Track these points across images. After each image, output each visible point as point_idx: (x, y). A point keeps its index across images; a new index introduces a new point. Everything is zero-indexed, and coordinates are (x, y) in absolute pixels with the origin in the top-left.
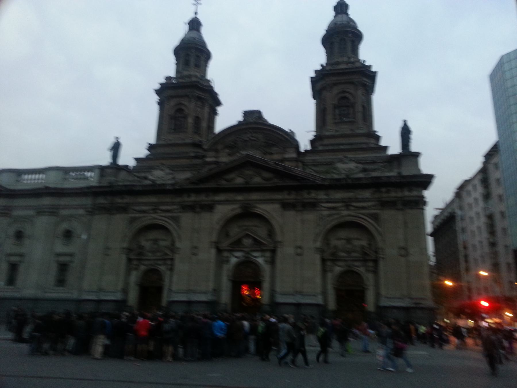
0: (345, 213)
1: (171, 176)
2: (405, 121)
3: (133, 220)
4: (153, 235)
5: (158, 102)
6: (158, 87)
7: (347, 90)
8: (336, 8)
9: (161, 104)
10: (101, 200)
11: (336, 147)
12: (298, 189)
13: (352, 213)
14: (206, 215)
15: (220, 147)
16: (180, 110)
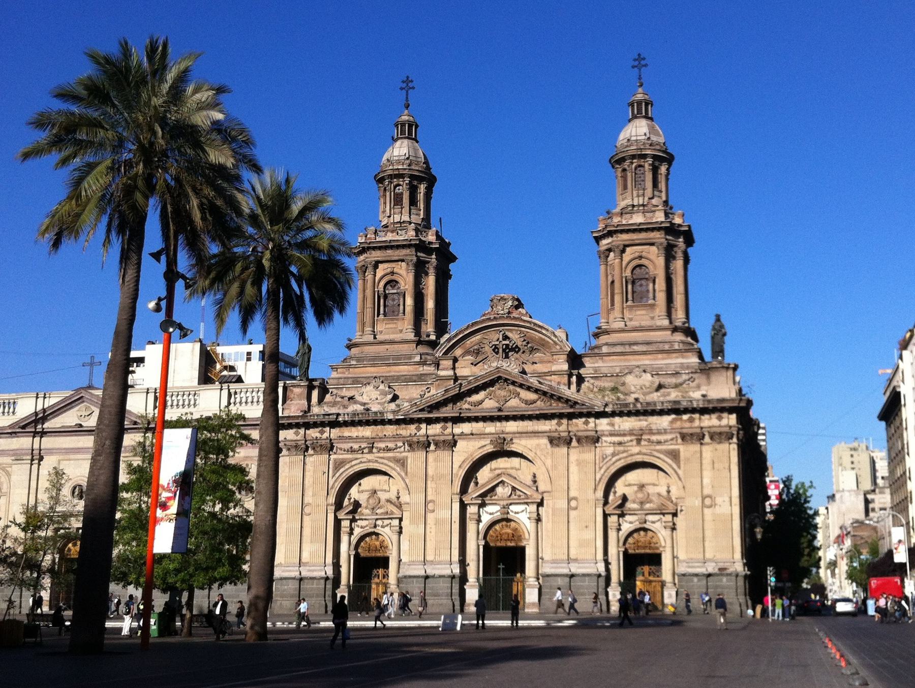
0: (636, 449)
1: (390, 397)
3: (339, 465)
4: (368, 482)
7: (644, 254)
11: (627, 349)
12: (570, 416)
13: (644, 451)
14: (444, 455)
15: (458, 352)
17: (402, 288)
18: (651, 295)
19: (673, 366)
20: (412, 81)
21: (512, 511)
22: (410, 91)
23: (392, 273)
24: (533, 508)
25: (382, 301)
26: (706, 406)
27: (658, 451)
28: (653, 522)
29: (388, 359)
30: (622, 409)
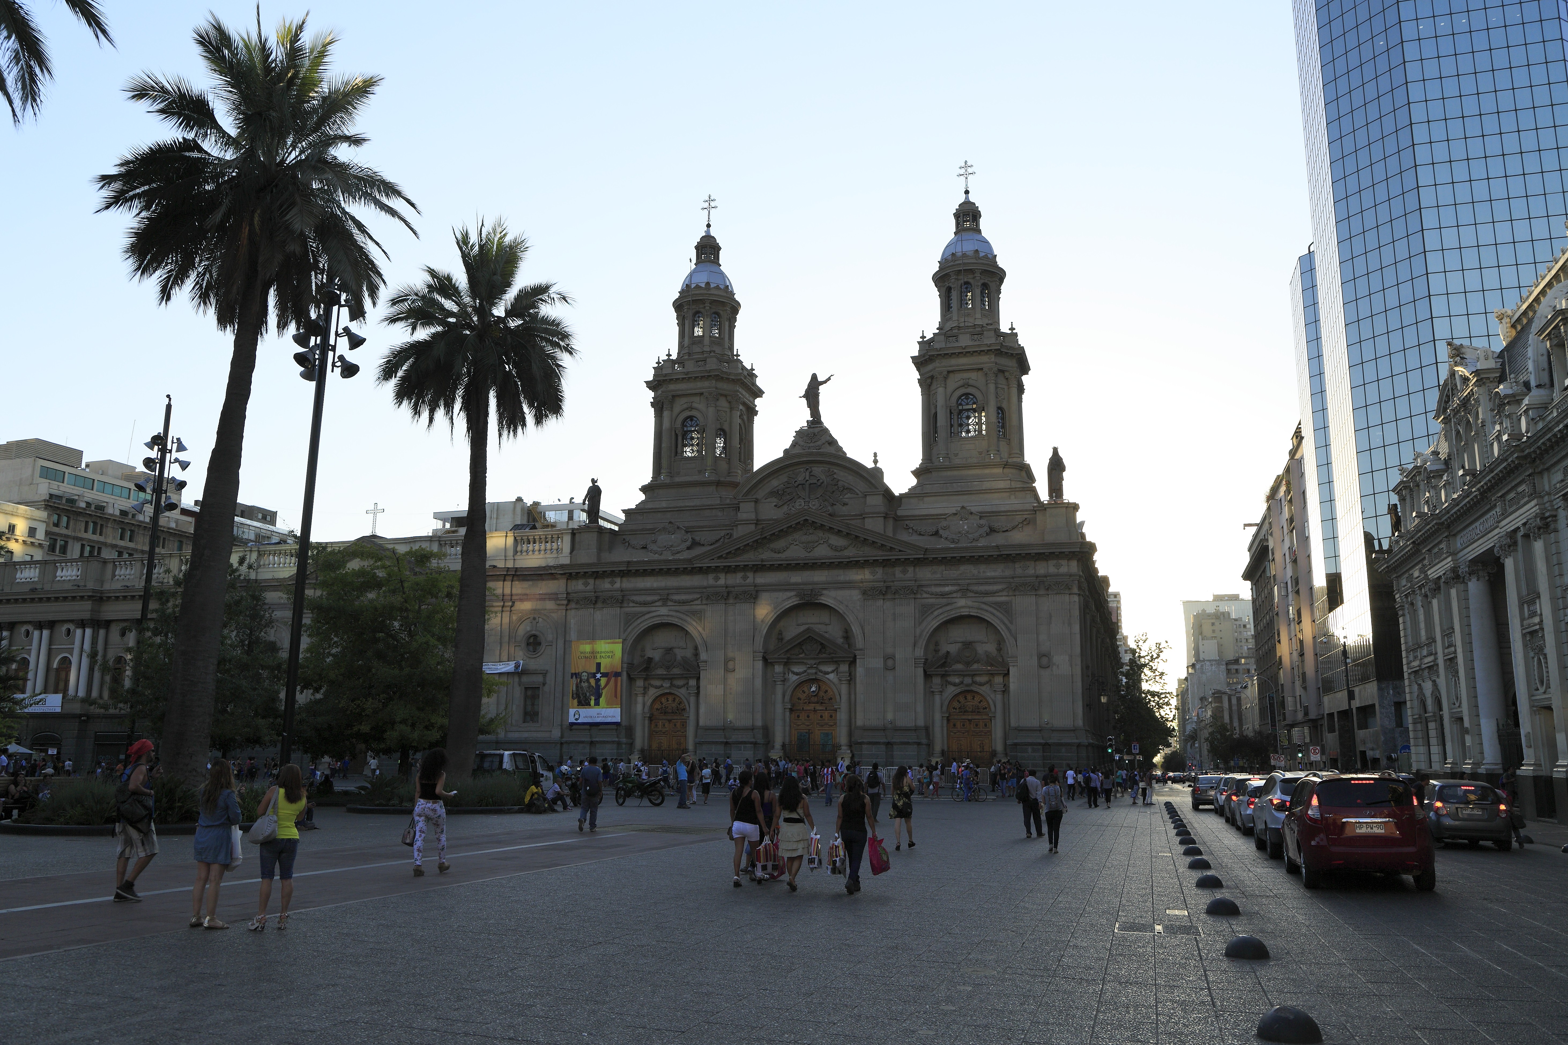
0: (962, 602)
2: (1055, 450)
7: (971, 382)
8: (957, 216)
10: (578, 585)
12: (886, 563)
13: (970, 603)
15: (760, 494)
21: (821, 671)
22: (712, 211)
24: (844, 668)
25: (680, 438)
27: (984, 603)
28: (981, 684)
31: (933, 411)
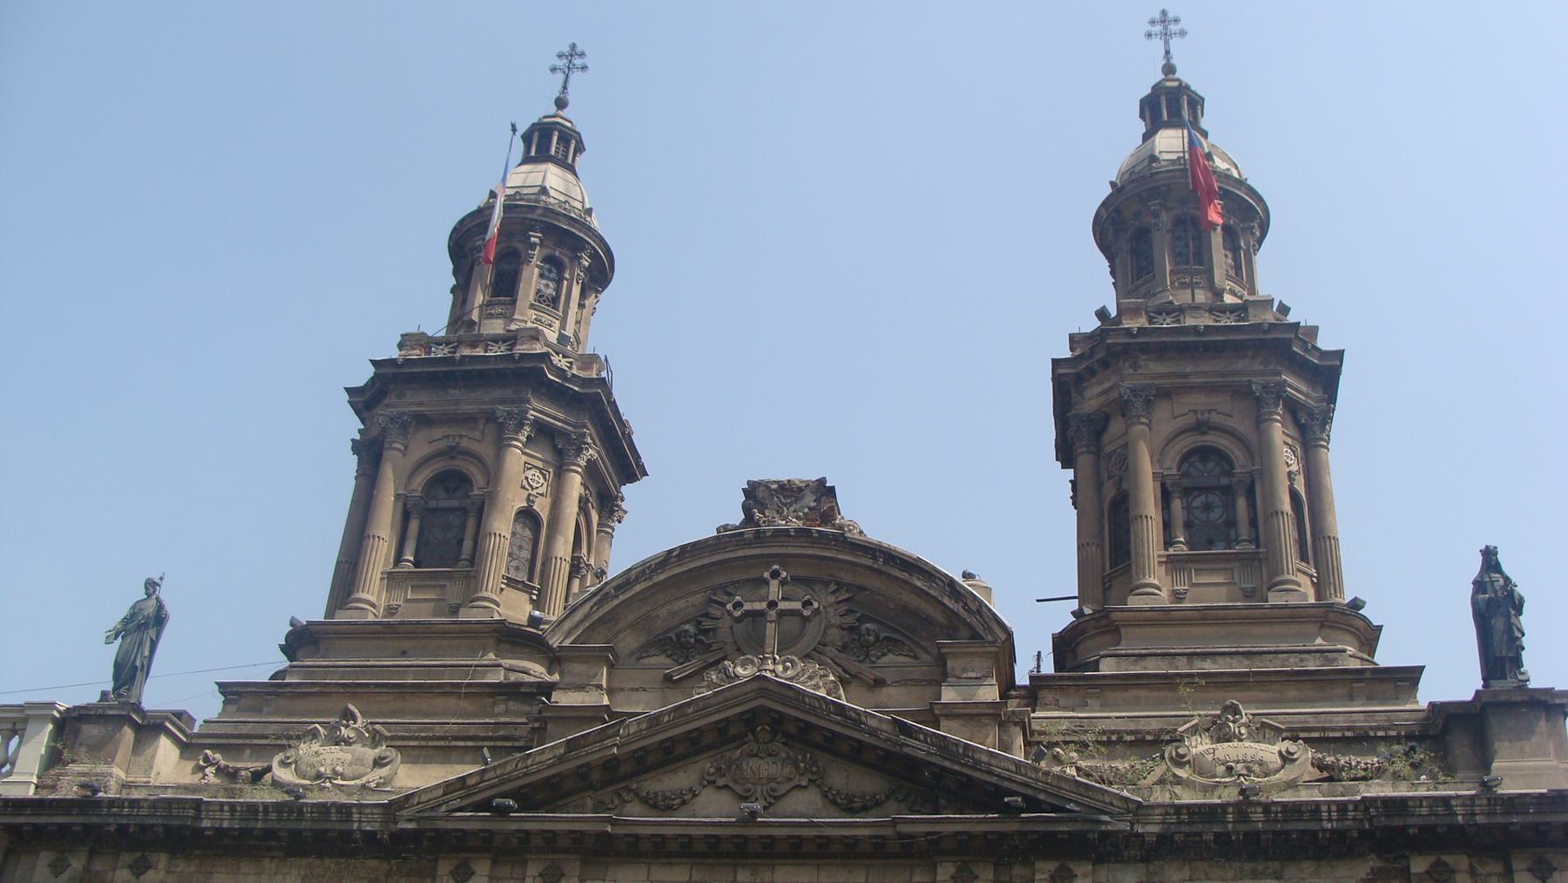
5: (353, 440)
6: (363, 375)
7: (1215, 418)
9: (370, 452)
16: (451, 481)
17: (476, 492)
18: (1244, 530)
19: (1341, 718)
20: (582, 55)
22: (576, 77)
23: (452, 452)
25: (414, 526)
26: (1500, 820)
29: (404, 675)
30: (1198, 828)
31: (1110, 492)
